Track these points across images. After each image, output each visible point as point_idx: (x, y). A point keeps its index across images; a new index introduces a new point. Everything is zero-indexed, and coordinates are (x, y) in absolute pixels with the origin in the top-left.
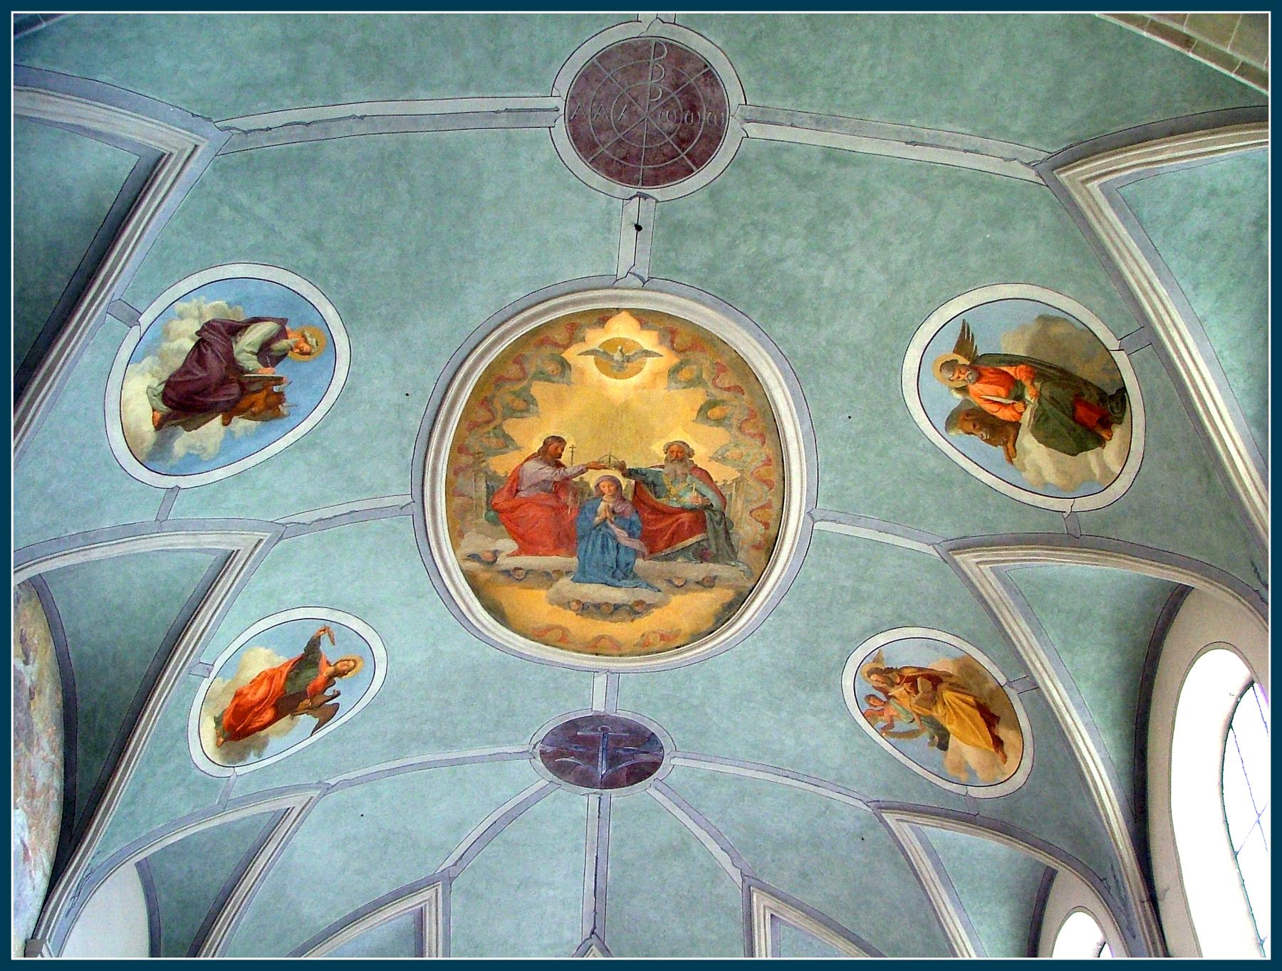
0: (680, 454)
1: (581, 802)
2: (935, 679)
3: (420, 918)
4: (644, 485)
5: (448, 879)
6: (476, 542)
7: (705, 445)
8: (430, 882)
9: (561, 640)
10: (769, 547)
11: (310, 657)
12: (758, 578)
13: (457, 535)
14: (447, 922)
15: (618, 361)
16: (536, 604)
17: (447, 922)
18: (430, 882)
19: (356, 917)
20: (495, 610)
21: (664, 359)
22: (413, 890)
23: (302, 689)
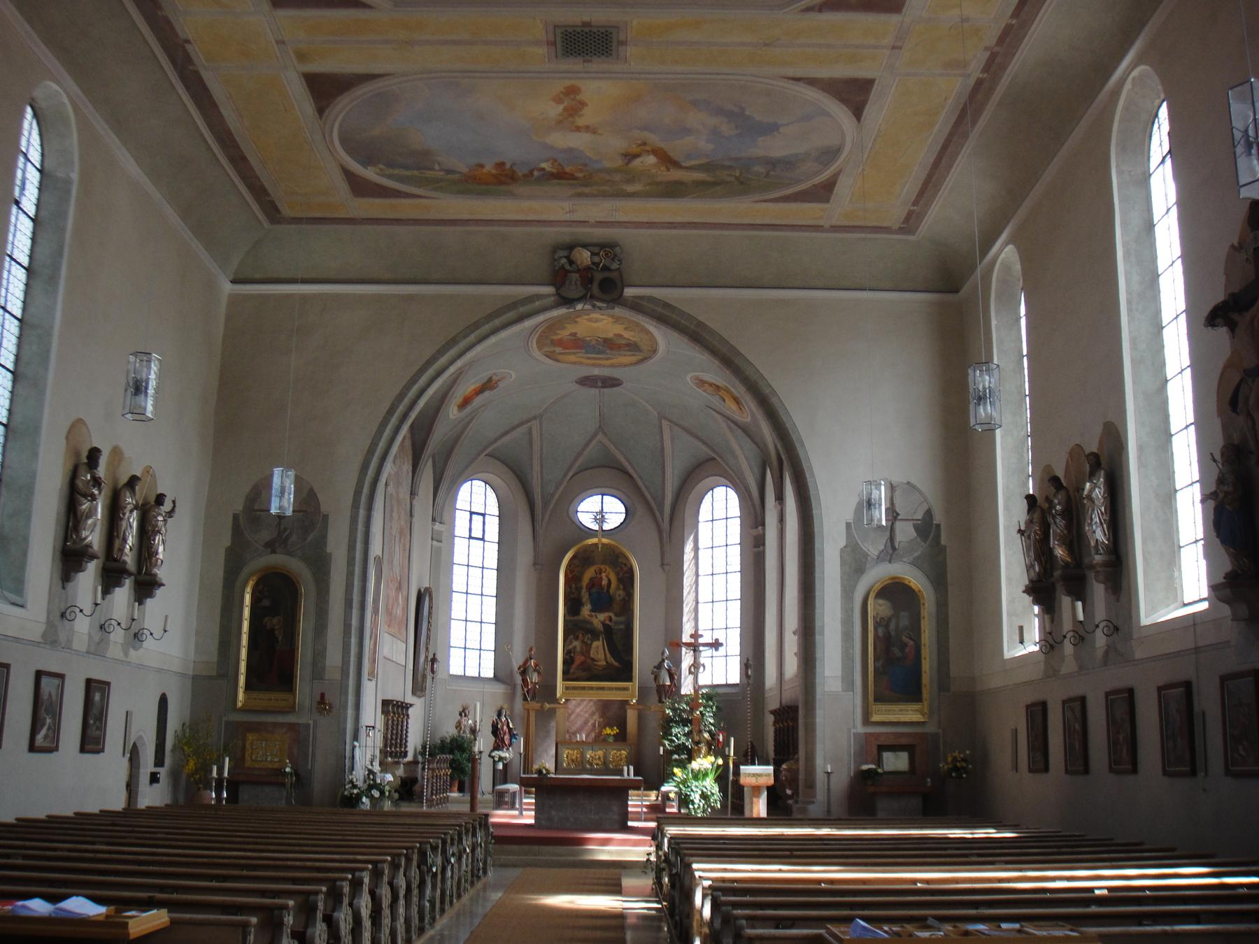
0: (620, 336)
1: (594, 392)
2: (718, 388)
3: (530, 430)
4: (605, 340)
5: (541, 416)
6: (546, 349)
7: (626, 334)
8: (535, 418)
9: (581, 363)
10: (655, 351)
11: (490, 380)
12: (650, 357)
13: (540, 348)
15: (597, 321)
16: (572, 358)
18: (535, 418)
19: (506, 433)
20: (558, 361)
21: (611, 320)
22: (528, 421)
23: (488, 385)
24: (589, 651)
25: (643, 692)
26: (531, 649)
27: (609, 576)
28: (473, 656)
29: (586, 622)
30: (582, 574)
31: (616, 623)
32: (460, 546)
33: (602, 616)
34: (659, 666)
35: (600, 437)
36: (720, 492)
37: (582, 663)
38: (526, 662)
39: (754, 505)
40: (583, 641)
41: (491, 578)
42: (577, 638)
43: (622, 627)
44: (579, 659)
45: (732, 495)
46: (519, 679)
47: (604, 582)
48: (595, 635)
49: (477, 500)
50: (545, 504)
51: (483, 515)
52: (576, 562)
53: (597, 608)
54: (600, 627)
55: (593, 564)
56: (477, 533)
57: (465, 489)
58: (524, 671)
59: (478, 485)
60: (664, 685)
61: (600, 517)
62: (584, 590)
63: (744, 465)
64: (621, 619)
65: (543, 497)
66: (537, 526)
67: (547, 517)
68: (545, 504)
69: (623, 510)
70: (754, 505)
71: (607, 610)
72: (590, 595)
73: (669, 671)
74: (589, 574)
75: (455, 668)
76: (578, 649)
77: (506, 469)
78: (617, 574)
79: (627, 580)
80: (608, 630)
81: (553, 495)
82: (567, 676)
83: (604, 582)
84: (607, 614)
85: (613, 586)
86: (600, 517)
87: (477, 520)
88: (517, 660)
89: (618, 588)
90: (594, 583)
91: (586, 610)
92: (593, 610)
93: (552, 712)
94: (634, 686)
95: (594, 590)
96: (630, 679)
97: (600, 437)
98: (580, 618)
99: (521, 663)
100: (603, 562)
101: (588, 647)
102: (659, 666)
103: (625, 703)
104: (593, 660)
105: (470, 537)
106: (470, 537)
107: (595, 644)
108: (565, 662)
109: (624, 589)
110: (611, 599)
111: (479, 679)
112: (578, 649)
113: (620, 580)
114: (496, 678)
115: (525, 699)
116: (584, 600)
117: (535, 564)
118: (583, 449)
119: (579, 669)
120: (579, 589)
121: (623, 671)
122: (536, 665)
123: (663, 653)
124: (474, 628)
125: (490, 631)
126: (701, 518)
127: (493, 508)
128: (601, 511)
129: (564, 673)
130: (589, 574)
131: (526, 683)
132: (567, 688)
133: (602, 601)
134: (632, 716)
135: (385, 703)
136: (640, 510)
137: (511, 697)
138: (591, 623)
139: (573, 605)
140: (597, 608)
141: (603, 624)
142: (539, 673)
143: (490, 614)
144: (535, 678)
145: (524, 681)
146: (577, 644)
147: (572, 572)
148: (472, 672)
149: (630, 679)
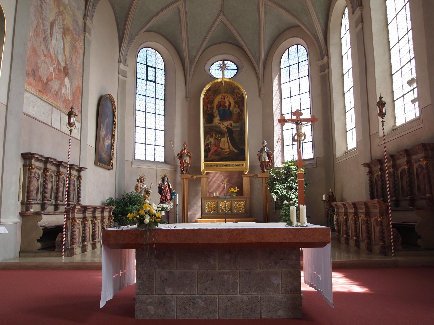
3: (179, 8)
14: (185, 9)
17: (185, 9)
24: (219, 143)
25: (252, 167)
26: (185, 143)
27: (230, 100)
28: (150, 149)
29: (216, 127)
30: (213, 100)
31: (234, 127)
32: (141, 85)
33: (226, 124)
34: (262, 151)
35: (221, 17)
36: (293, 49)
37: (216, 151)
38: (182, 151)
39: (320, 46)
40: (215, 138)
41: (161, 105)
42: (212, 137)
43: (238, 129)
44: (213, 149)
45: (303, 51)
46: (179, 161)
47: (227, 104)
48: (222, 134)
49: (150, 59)
50: (191, 63)
51: (155, 68)
52: (210, 93)
53: (223, 118)
54: (226, 130)
55: (220, 93)
56: (151, 77)
57: (142, 54)
58: (181, 156)
59: (151, 51)
60: (265, 162)
61: (223, 68)
62: (215, 109)
63: (314, 18)
64: (237, 124)
65: (189, 58)
66: (187, 76)
67: (193, 68)
68: (191, 63)
69: (235, 67)
70: (320, 46)
71: (229, 120)
72: (219, 111)
73: (267, 153)
74: (217, 100)
75: (139, 156)
76: (213, 143)
77: (167, 42)
78: (234, 99)
79: (240, 102)
80: (230, 131)
81: (195, 57)
82: (206, 159)
83: (227, 104)
84: (229, 122)
85: (232, 105)
86: (223, 68)
87: (151, 71)
88: (177, 149)
89: (235, 107)
90: (220, 105)
91: (217, 120)
92: (220, 120)
93: (199, 180)
94: (247, 164)
95: (221, 108)
96: (244, 159)
97: (221, 17)
98: (213, 124)
99: (179, 152)
100: (225, 93)
101: (219, 142)
102: (262, 151)
103: (242, 173)
104: (222, 149)
105: (147, 80)
106: (147, 80)
107: (223, 139)
108: (205, 151)
109: (239, 107)
110: (231, 113)
111: (155, 162)
112: (213, 143)
113: (236, 102)
114: (165, 162)
115: (182, 173)
116: (215, 114)
117: (186, 97)
118: (212, 26)
119: (214, 155)
120: (212, 108)
121: (239, 154)
122: (188, 153)
123: (263, 143)
124: (150, 133)
125: (161, 136)
126: (282, 66)
127: (161, 64)
128: (222, 71)
129: (205, 157)
130: (217, 100)
131: (183, 164)
132: (207, 166)
133: (226, 115)
134: (246, 181)
135: (27, 157)
136: (246, 66)
137: (174, 172)
138: (220, 127)
139: (209, 118)
140: (223, 118)
141: (227, 128)
142: (190, 157)
143: (161, 124)
144: (188, 160)
145: (181, 162)
146: (212, 140)
147: (208, 98)
148: (150, 158)
149: (244, 159)
